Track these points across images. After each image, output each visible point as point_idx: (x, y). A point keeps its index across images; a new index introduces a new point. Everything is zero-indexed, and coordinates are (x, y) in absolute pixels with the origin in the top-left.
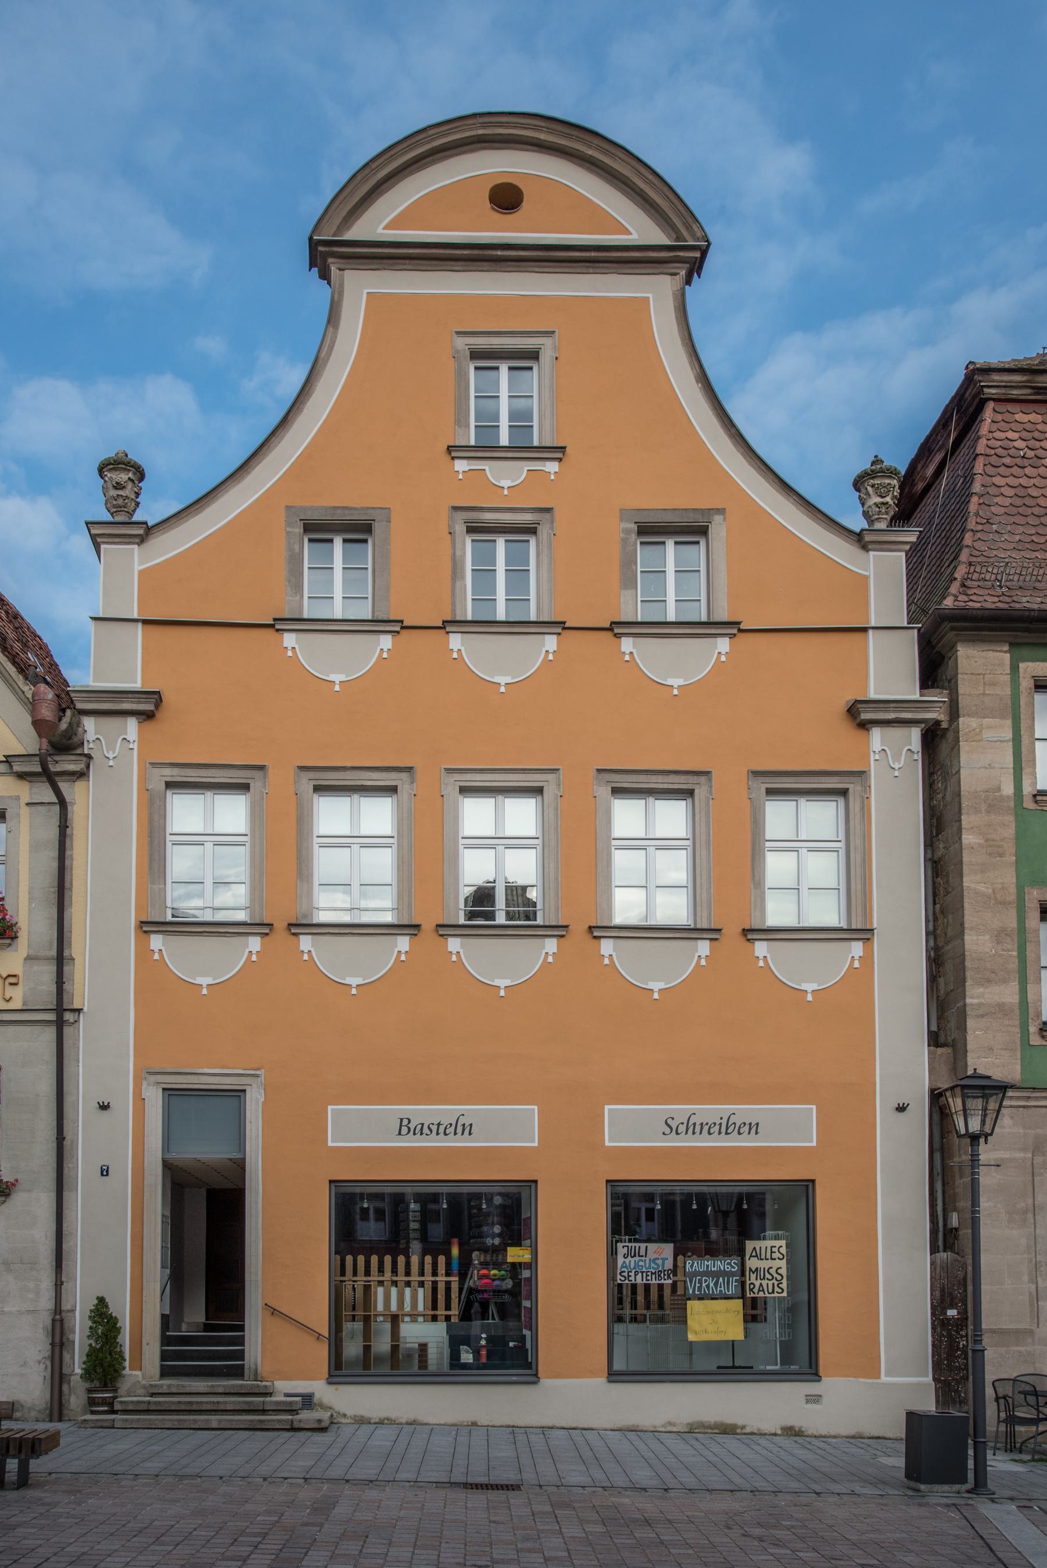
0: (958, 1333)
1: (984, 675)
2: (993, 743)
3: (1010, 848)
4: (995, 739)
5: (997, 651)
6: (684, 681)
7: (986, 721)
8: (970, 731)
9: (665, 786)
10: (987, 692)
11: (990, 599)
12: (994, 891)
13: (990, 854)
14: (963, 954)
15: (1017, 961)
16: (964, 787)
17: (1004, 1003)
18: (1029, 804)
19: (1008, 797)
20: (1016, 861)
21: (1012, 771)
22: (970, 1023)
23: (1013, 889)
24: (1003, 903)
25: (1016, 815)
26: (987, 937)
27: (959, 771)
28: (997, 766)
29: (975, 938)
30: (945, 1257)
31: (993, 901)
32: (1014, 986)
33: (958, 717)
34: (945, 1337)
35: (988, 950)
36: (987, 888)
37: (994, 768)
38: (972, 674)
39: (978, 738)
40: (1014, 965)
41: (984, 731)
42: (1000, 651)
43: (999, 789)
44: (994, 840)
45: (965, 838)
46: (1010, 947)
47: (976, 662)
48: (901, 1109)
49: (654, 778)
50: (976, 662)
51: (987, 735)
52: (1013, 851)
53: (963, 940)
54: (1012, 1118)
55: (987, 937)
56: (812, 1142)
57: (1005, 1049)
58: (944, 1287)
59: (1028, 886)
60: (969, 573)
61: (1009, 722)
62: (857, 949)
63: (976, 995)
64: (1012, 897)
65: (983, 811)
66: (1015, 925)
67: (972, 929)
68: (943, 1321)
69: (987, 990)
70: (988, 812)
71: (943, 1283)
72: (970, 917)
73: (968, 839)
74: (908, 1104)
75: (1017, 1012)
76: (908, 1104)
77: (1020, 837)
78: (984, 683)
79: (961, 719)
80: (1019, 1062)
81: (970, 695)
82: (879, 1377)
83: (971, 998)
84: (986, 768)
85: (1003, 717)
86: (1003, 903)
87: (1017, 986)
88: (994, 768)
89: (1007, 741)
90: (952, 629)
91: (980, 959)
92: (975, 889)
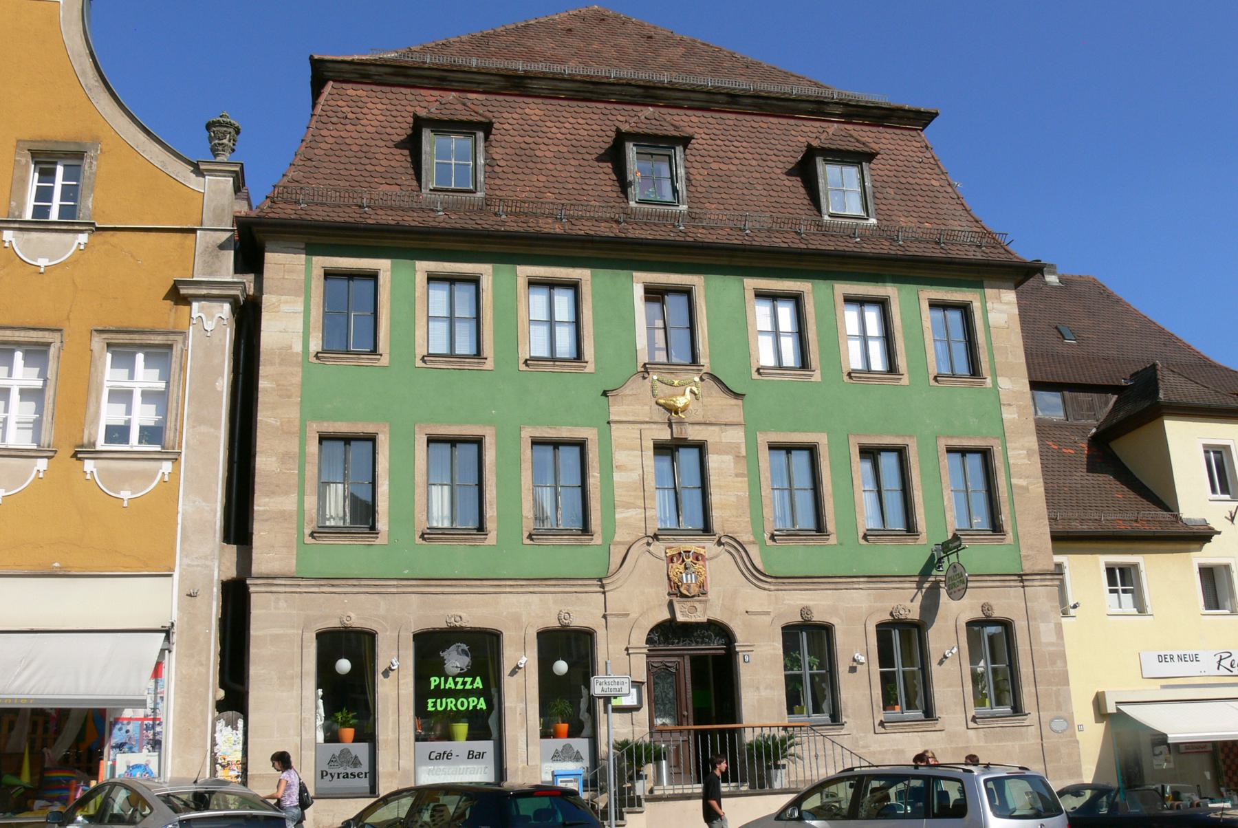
6: (49, 261)
9: (26, 339)
10: (286, 277)
12: (281, 424)
13: (280, 396)
15: (297, 478)
19: (297, 354)
20: (301, 401)
23: (297, 423)
25: (303, 367)
26: (274, 459)
32: (294, 497)
43: (291, 347)
44: (283, 385)
49: (17, 333)
51: (284, 308)
52: (299, 394)
54: (286, 601)
55: (274, 459)
61: (302, 299)
62: (167, 467)
66: (297, 450)
70: (280, 364)
77: (302, 384)
84: (280, 332)
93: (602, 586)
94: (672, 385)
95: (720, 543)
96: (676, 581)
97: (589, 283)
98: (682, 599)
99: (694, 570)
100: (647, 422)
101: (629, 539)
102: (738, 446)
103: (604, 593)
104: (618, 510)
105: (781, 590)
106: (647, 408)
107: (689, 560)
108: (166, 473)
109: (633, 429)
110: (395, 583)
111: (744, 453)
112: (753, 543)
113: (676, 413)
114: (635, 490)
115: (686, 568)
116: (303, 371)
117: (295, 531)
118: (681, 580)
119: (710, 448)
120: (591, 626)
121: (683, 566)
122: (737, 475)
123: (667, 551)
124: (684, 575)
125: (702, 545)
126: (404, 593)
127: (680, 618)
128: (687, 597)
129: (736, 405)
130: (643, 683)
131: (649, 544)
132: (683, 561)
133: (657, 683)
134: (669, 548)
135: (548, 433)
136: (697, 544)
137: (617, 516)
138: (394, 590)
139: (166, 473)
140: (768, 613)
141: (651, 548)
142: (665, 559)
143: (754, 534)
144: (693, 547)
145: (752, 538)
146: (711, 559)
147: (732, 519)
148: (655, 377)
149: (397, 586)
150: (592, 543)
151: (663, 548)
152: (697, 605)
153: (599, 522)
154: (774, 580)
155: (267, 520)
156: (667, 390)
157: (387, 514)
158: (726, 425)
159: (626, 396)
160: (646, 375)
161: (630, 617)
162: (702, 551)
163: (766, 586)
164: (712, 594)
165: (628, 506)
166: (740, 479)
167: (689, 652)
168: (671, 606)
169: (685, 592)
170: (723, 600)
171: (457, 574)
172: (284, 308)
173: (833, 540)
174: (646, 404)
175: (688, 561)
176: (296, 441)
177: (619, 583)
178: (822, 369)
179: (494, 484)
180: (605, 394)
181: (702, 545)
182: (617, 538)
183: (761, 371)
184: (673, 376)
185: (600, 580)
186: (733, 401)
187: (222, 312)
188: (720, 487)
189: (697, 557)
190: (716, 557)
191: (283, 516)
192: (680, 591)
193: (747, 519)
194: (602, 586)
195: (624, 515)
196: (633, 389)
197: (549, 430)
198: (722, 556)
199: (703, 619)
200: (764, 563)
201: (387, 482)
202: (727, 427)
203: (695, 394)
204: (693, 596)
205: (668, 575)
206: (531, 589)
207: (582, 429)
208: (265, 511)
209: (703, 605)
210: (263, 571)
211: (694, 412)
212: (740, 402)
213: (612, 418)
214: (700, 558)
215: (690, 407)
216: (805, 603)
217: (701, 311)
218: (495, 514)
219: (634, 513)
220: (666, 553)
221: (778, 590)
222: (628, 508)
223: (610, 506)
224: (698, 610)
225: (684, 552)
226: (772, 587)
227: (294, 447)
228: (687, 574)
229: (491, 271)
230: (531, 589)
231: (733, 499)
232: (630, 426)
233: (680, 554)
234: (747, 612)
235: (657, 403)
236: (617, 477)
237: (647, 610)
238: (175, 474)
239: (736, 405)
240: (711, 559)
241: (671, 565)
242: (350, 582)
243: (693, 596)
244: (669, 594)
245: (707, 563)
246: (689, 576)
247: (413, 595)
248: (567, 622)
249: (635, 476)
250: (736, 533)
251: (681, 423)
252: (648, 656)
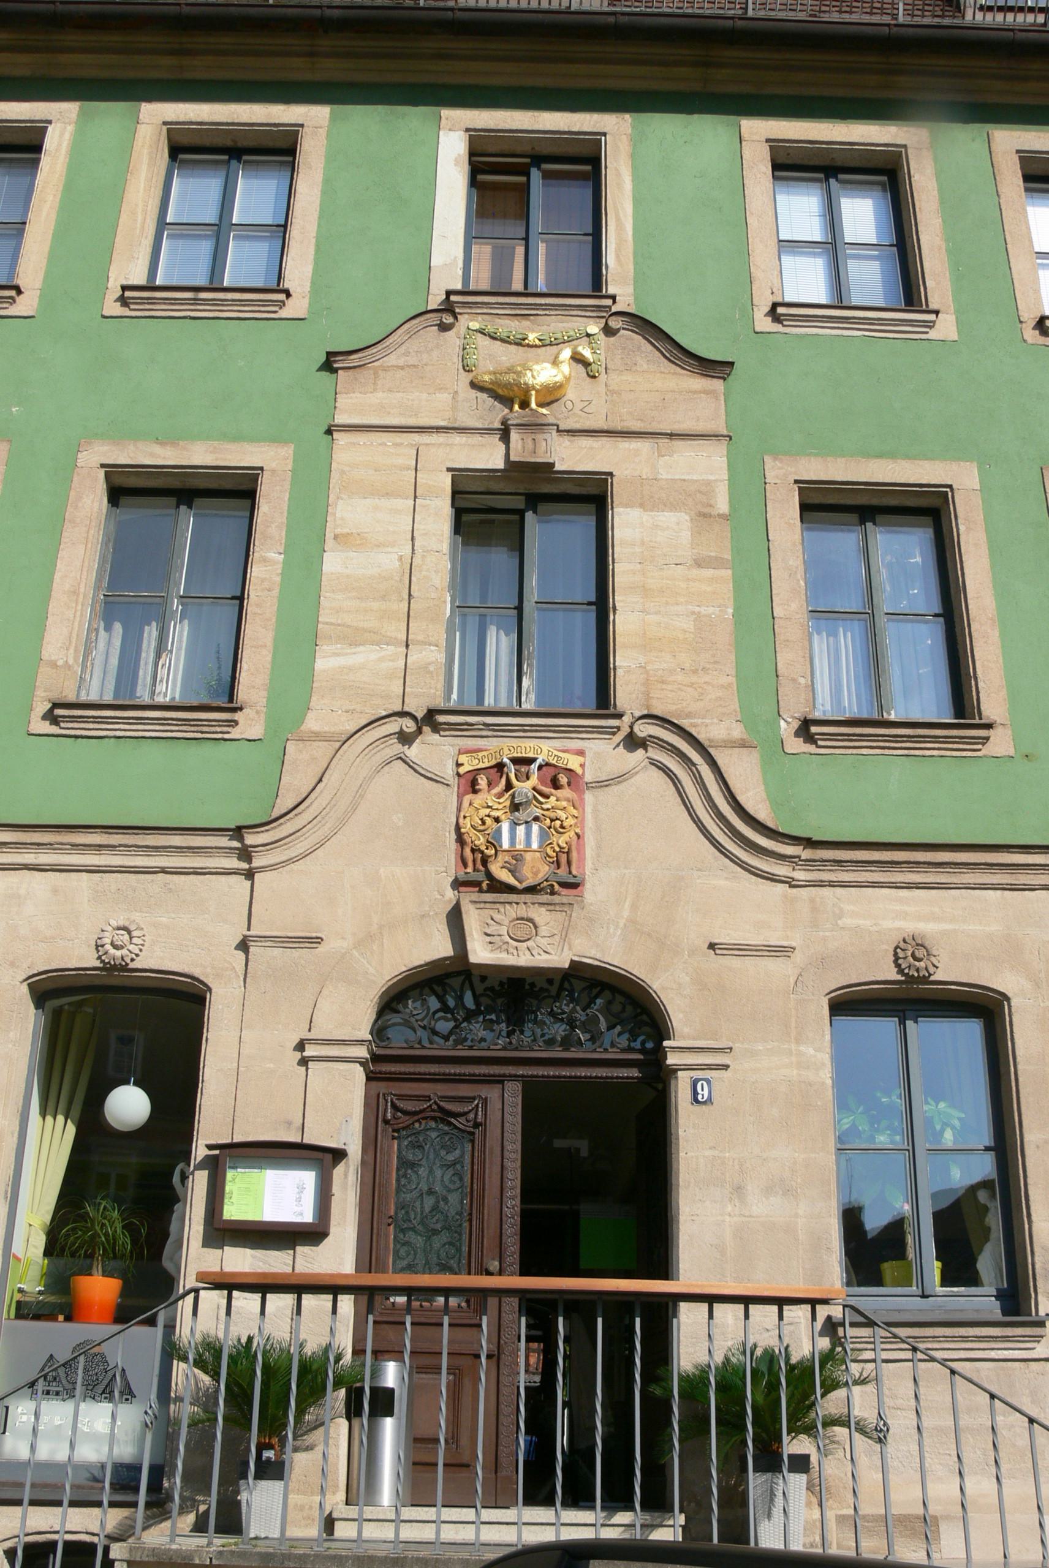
93: (245, 854)
94: (520, 342)
95: (633, 742)
96: (481, 842)
97: (323, 132)
98: (489, 897)
99: (538, 812)
100: (438, 429)
102: (706, 489)
103: (250, 875)
104: (324, 648)
105: (832, 884)
106: (445, 397)
107: (529, 784)
109: (396, 445)
111: (722, 505)
112: (743, 745)
113: (524, 405)
114: (383, 598)
115: (515, 807)
118: (494, 843)
119: (619, 492)
120: (197, 972)
121: (506, 800)
122: (699, 563)
123: (463, 759)
124: (505, 827)
127: (480, 953)
128: (510, 889)
129: (706, 392)
130: (338, 1155)
131: (405, 739)
132: (509, 786)
133: (413, 1165)
134: (467, 752)
135: (152, 455)
136: (557, 743)
137: (320, 664)
140: (782, 951)
141: (414, 752)
142: (454, 781)
143: (746, 718)
144: (544, 750)
145: (737, 732)
146: (602, 784)
147: (680, 677)
148: (475, 325)
150: (235, 733)
151: (453, 751)
152: (541, 915)
153: (262, 679)
154: (807, 854)
156: (507, 355)
158: (671, 436)
159: (386, 369)
160: (448, 319)
161: (322, 949)
162: (573, 763)
163: (781, 870)
164: (594, 891)
165: (354, 638)
166: (709, 573)
167: (521, 1071)
168: (455, 919)
169: (505, 876)
170: (634, 907)
173: (1000, 743)
174: (441, 389)
175: (525, 788)
178: (959, 313)
180: (329, 365)
182: (312, 723)
183: (781, 310)
184: (526, 323)
185: (238, 832)
186: (698, 383)
188: (645, 591)
190: (620, 778)
192: (489, 875)
193: (724, 680)
194: (245, 854)
195: (342, 661)
196: (407, 354)
197: (157, 449)
198: (637, 780)
199: (558, 958)
200: (775, 804)
202: (678, 444)
203: (586, 364)
204: (532, 890)
205: (458, 828)
206: (29, 858)
207: (248, 447)
209: (560, 916)
211: (580, 405)
212: (718, 385)
213: (340, 419)
214: (563, 779)
215: (571, 394)
216: (910, 926)
217: (620, 186)
219: (374, 656)
220: (458, 765)
221: (820, 884)
222: (354, 644)
224: (544, 930)
225: (516, 761)
226: (800, 875)
228: (515, 824)
229: (74, 116)
230: (29, 858)
231: (688, 624)
232: (389, 438)
233: (500, 766)
234: (712, 946)
235: (474, 385)
236: (333, 562)
237: (381, 927)
239: (706, 392)
240: (602, 784)
241: (467, 798)
243: (532, 890)
244: (457, 884)
245: (589, 797)
246: (521, 830)
248: (118, 953)
249: (389, 561)
250: (689, 715)
251: (535, 426)
252: (370, 1078)
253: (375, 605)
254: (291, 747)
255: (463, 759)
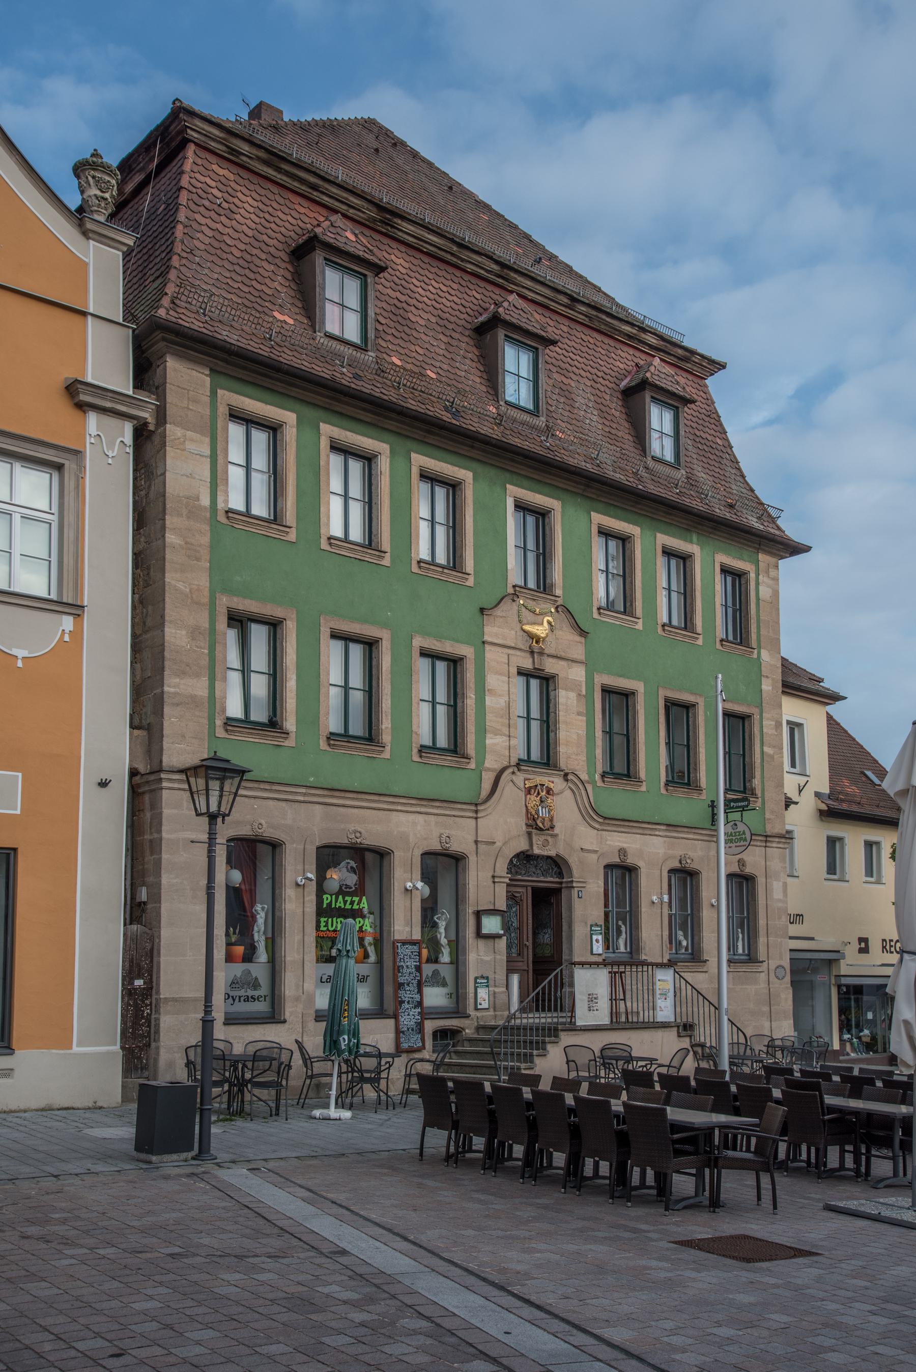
0: (143, 1002)
1: (188, 390)
2: (194, 456)
3: (205, 554)
4: (196, 452)
5: (200, 372)
7: (189, 433)
8: (175, 439)
11: (197, 323)
12: (190, 591)
13: (189, 557)
14: (163, 645)
15: (207, 659)
16: (169, 489)
17: (196, 696)
18: (222, 518)
19: (205, 508)
21: (209, 485)
22: (167, 710)
23: (206, 593)
24: (198, 603)
25: (211, 526)
26: (184, 632)
27: (164, 474)
28: (197, 477)
29: (174, 631)
30: (135, 929)
31: (189, 600)
33: (165, 423)
34: (131, 1006)
35: (184, 644)
36: (186, 587)
37: (194, 478)
38: (178, 386)
39: (182, 447)
40: (205, 662)
41: (186, 443)
42: (203, 373)
44: (192, 544)
45: (168, 537)
46: (202, 645)
47: (182, 376)
48: (103, 784)
50: (182, 376)
52: (208, 558)
53: (163, 631)
56: (16, 809)
57: (196, 738)
58: (133, 958)
59: (219, 592)
60: (178, 293)
63: (172, 685)
64: (206, 600)
65: (184, 514)
66: (207, 625)
67: (171, 622)
68: (131, 991)
69: (182, 682)
71: (133, 955)
72: (171, 611)
73: (171, 538)
74: (110, 781)
75: (206, 704)
76: (110, 781)
77: (214, 546)
78: (188, 398)
79: (168, 426)
80: (207, 750)
81: (177, 406)
82: (71, 1048)
83: (169, 686)
85: (202, 434)
86: (198, 603)
87: (207, 682)
88: (194, 478)
89: (206, 457)
90: (164, 339)
91: (177, 652)
92: (175, 586)
96: (533, 813)
101: (498, 766)
104: (488, 735)
108: (67, 631)
110: (303, 790)
116: (211, 530)
117: (206, 721)
123: (526, 782)
124: (540, 808)
125: (551, 779)
126: (310, 802)
137: (488, 742)
138: (301, 798)
139: (67, 631)
142: (524, 790)
147: (574, 757)
149: (305, 794)
151: (523, 778)
155: (178, 705)
157: (294, 714)
162: (551, 785)
171: (357, 786)
172: (190, 446)
176: (206, 614)
177: (489, 810)
179: (389, 693)
181: (551, 779)
187: (124, 437)
189: (549, 791)
191: (193, 701)
201: (294, 677)
206: (418, 809)
208: (176, 694)
210: (175, 764)
218: (390, 726)
223: (482, 731)
227: (204, 621)
228: (542, 808)
230: (418, 809)
233: (536, 786)
238: (77, 634)
241: (528, 796)
242: (262, 786)
247: (317, 806)
253: (500, 720)
254: (483, 773)
255: (526, 782)
